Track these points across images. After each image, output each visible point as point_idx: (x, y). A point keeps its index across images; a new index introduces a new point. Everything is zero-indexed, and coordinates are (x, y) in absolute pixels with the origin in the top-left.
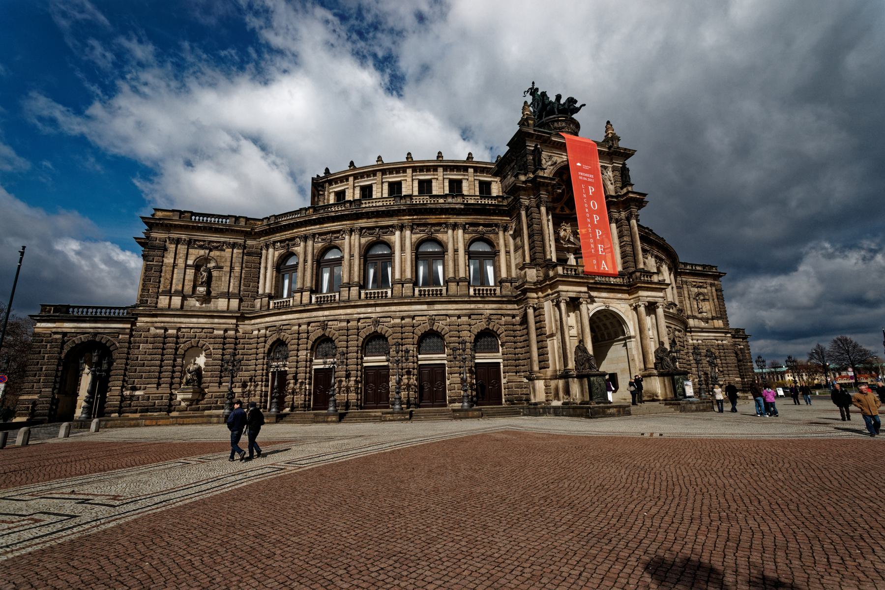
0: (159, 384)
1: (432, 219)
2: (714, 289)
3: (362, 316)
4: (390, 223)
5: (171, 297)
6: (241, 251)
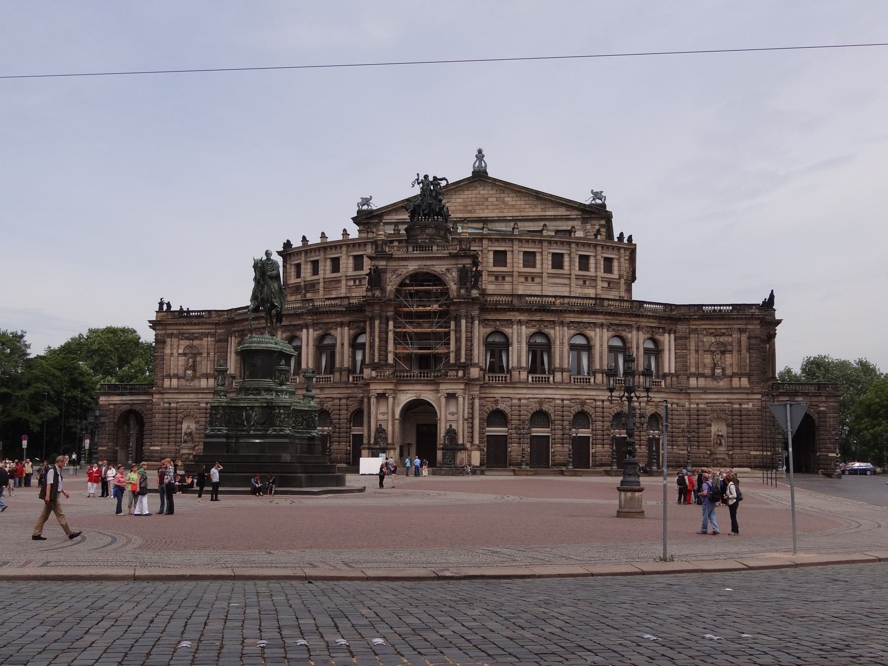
0: (169, 442)
2: (744, 337)
4: (299, 322)
5: (171, 379)
6: (213, 339)
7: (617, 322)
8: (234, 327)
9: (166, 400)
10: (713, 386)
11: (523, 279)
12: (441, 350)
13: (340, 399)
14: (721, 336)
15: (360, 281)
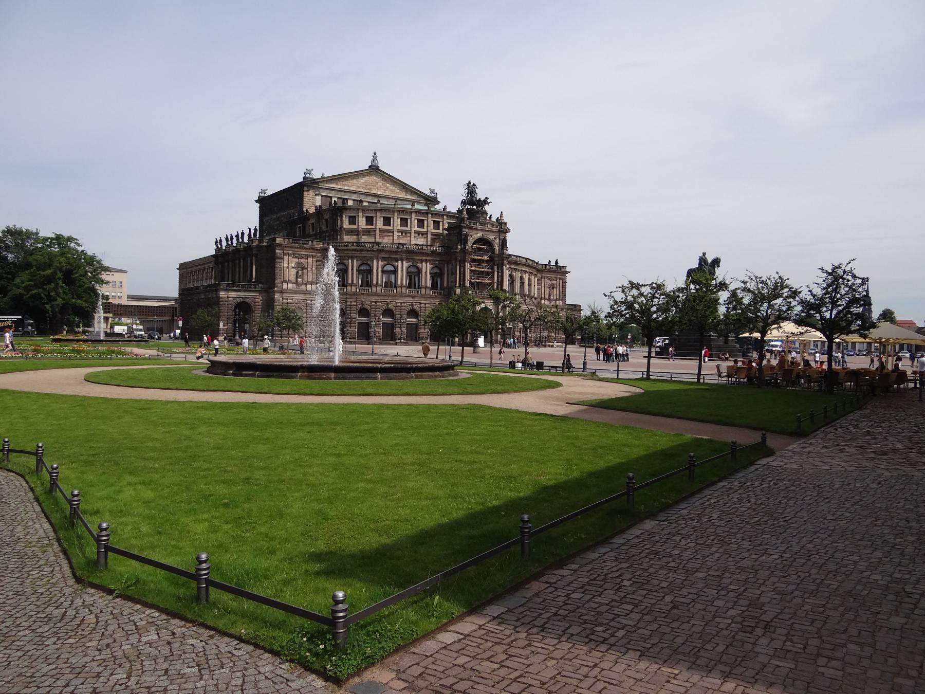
2: (561, 281)
4: (396, 257)
12: (487, 281)
13: (425, 304)
15: (406, 234)
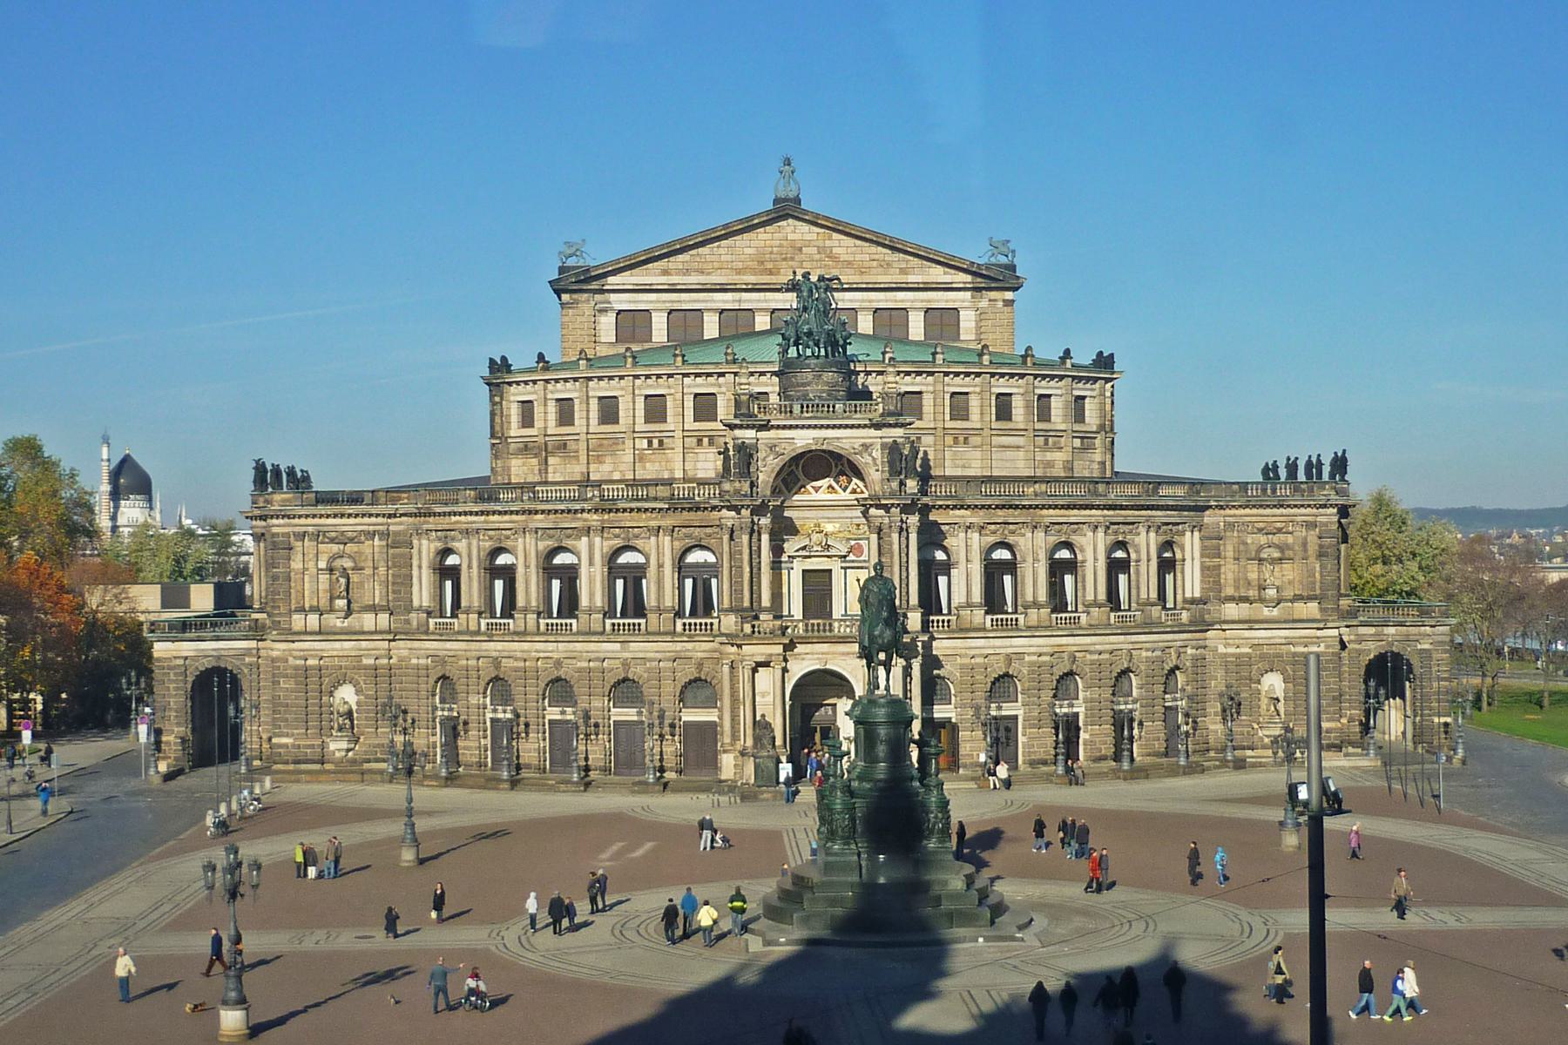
1: (627, 519)
2: (1312, 536)
3: (542, 655)
6: (384, 543)
7: (1121, 520)
8: (428, 523)
9: (298, 653)
10: (1261, 618)
11: (949, 440)
14: (1274, 534)
15: (661, 443)
